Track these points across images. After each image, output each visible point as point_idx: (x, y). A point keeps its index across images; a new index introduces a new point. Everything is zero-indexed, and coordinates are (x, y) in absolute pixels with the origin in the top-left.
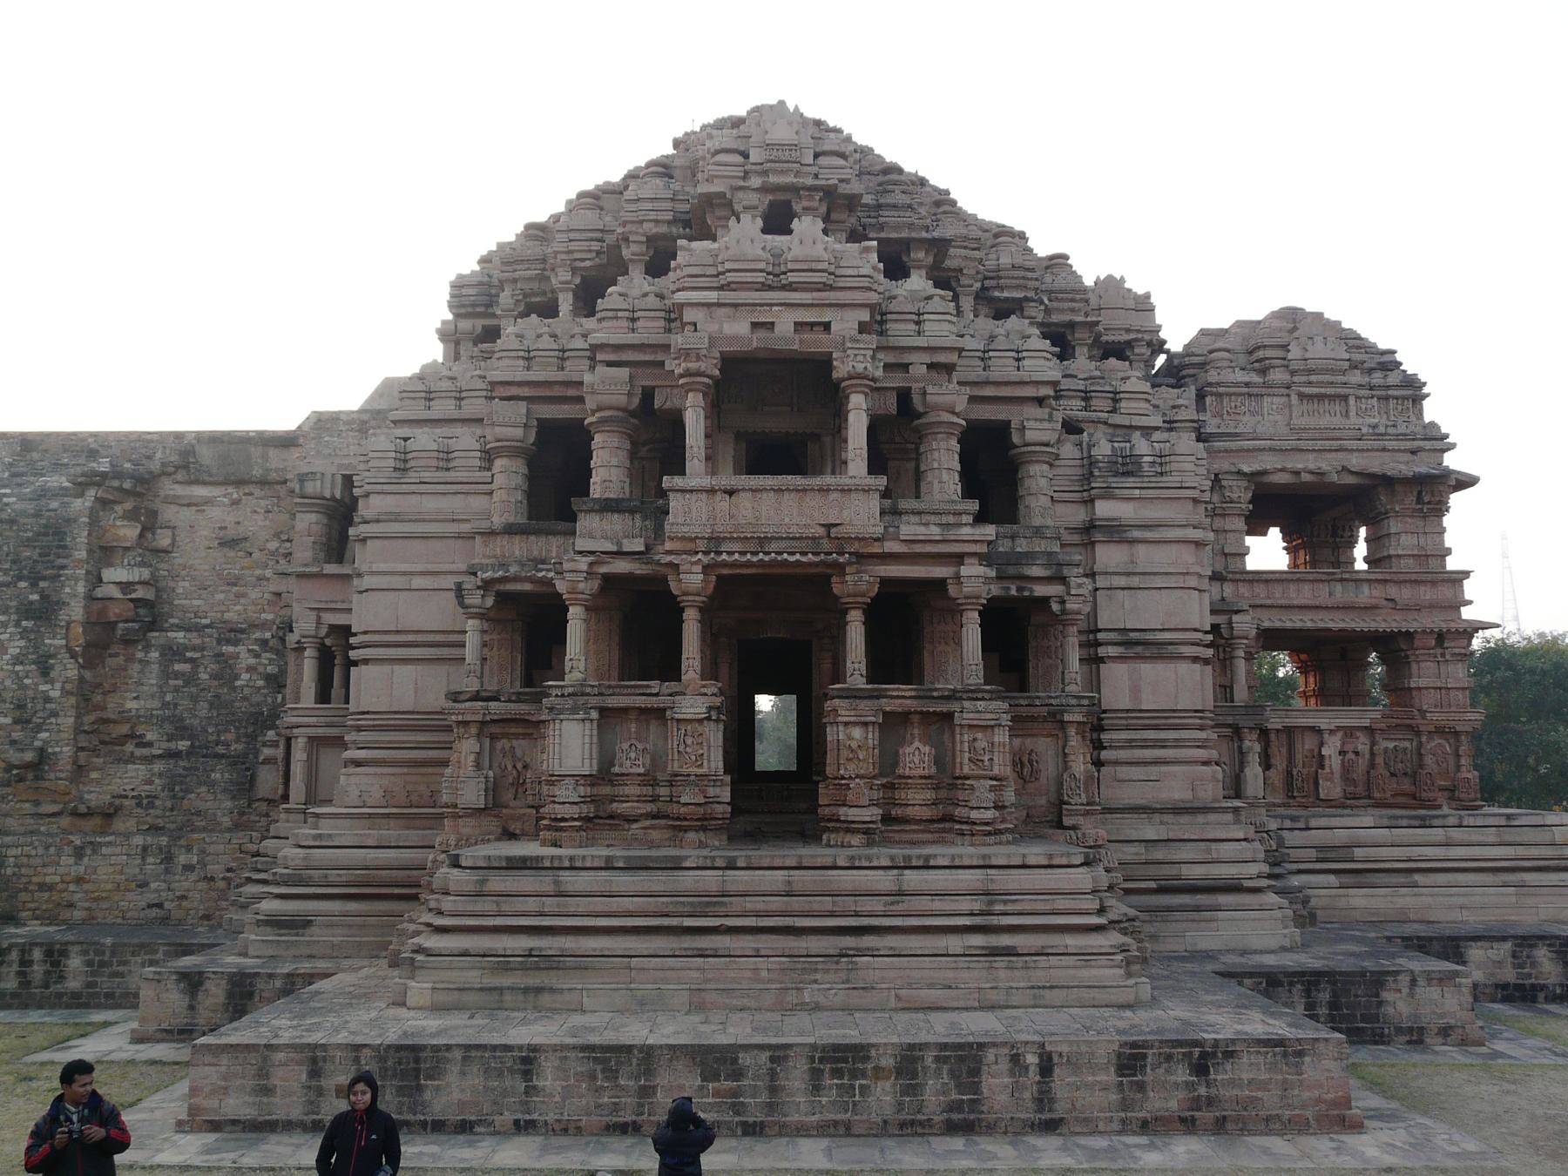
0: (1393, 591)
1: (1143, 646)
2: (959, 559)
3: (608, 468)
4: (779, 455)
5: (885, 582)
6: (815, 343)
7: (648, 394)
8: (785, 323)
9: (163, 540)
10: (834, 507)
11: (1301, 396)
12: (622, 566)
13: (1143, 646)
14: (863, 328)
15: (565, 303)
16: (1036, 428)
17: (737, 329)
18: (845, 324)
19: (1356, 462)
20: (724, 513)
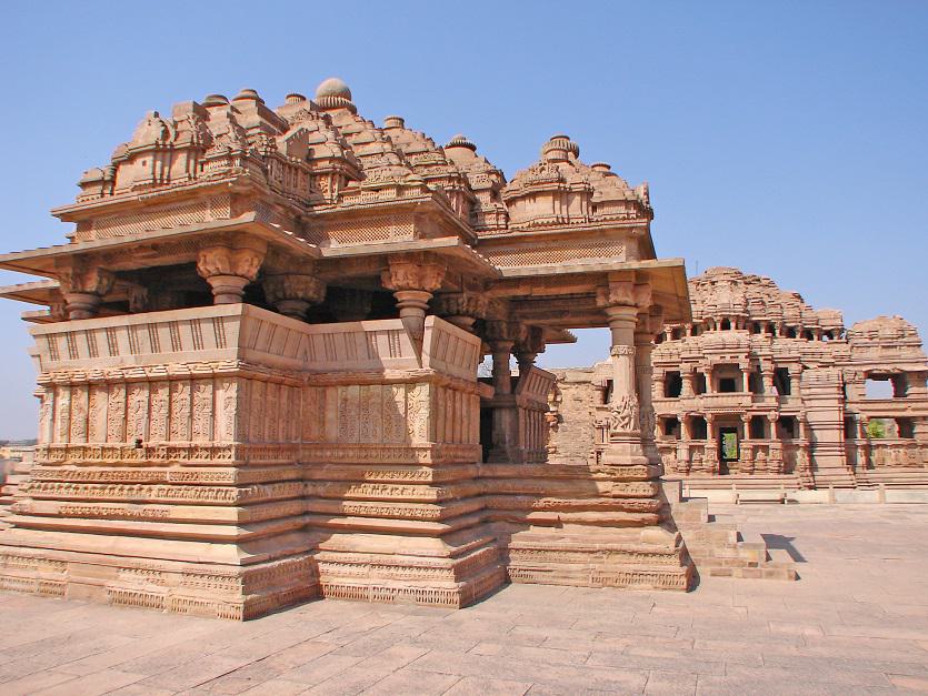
0: (909, 404)
1: (825, 426)
2: (770, 411)
3: (686, 386)
4: (727, 386)
5: (753, 416)
6: (735, 361)
7: (695, 369)
8: (728, 356)
9: (558, 399)
10: (740, 401)
11: (883, 347)
12: (693, 414)
13: (825, 426)
14: (746, 357)
15: (669, 336)
16: (793, 369)
17: (717, 359)
18: (742, 356)
19: (899, 366)
20: (712, 402)
